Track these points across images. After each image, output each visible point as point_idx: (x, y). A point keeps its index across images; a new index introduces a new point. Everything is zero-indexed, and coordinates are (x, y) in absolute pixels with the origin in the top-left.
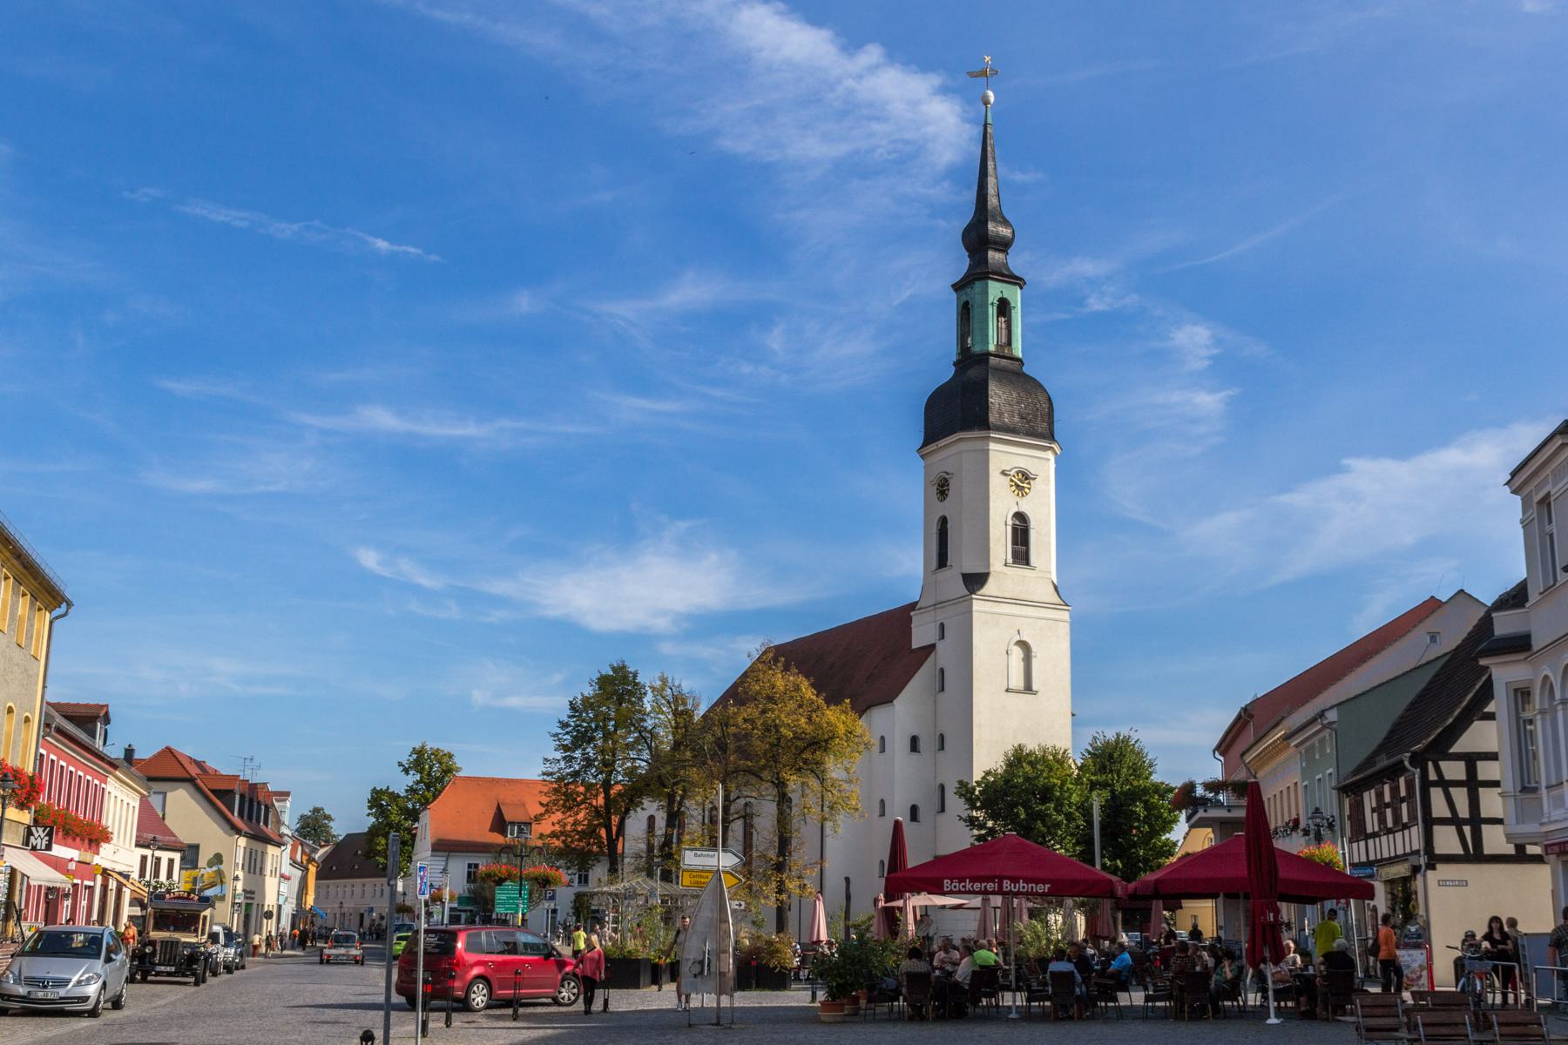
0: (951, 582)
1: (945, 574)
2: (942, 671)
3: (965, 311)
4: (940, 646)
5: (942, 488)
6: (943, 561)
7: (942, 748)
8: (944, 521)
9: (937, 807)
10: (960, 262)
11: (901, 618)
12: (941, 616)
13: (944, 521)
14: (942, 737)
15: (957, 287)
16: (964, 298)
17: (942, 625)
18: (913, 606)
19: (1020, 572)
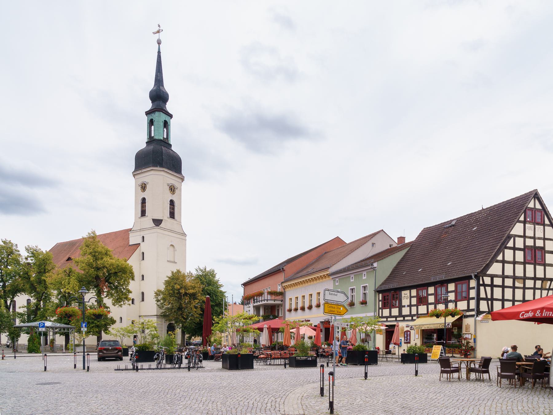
0: (147, 222)
1: (144, 219)
2: (143, 253)
3: (151, 123)
4: (142, 244)
5: (144, 187)
6: (143, 213)
7: (143, 279)
8: (144, 201)
9: (141, 299)
10: (149, 105)
11: (126, 233)
12: (142, 234)
13: (144, 201)
14: (143, 276)
15: (147, 113)
16: (151, 118)
17: (143, 237)
18: (130, 230)
19: (171, 220)
